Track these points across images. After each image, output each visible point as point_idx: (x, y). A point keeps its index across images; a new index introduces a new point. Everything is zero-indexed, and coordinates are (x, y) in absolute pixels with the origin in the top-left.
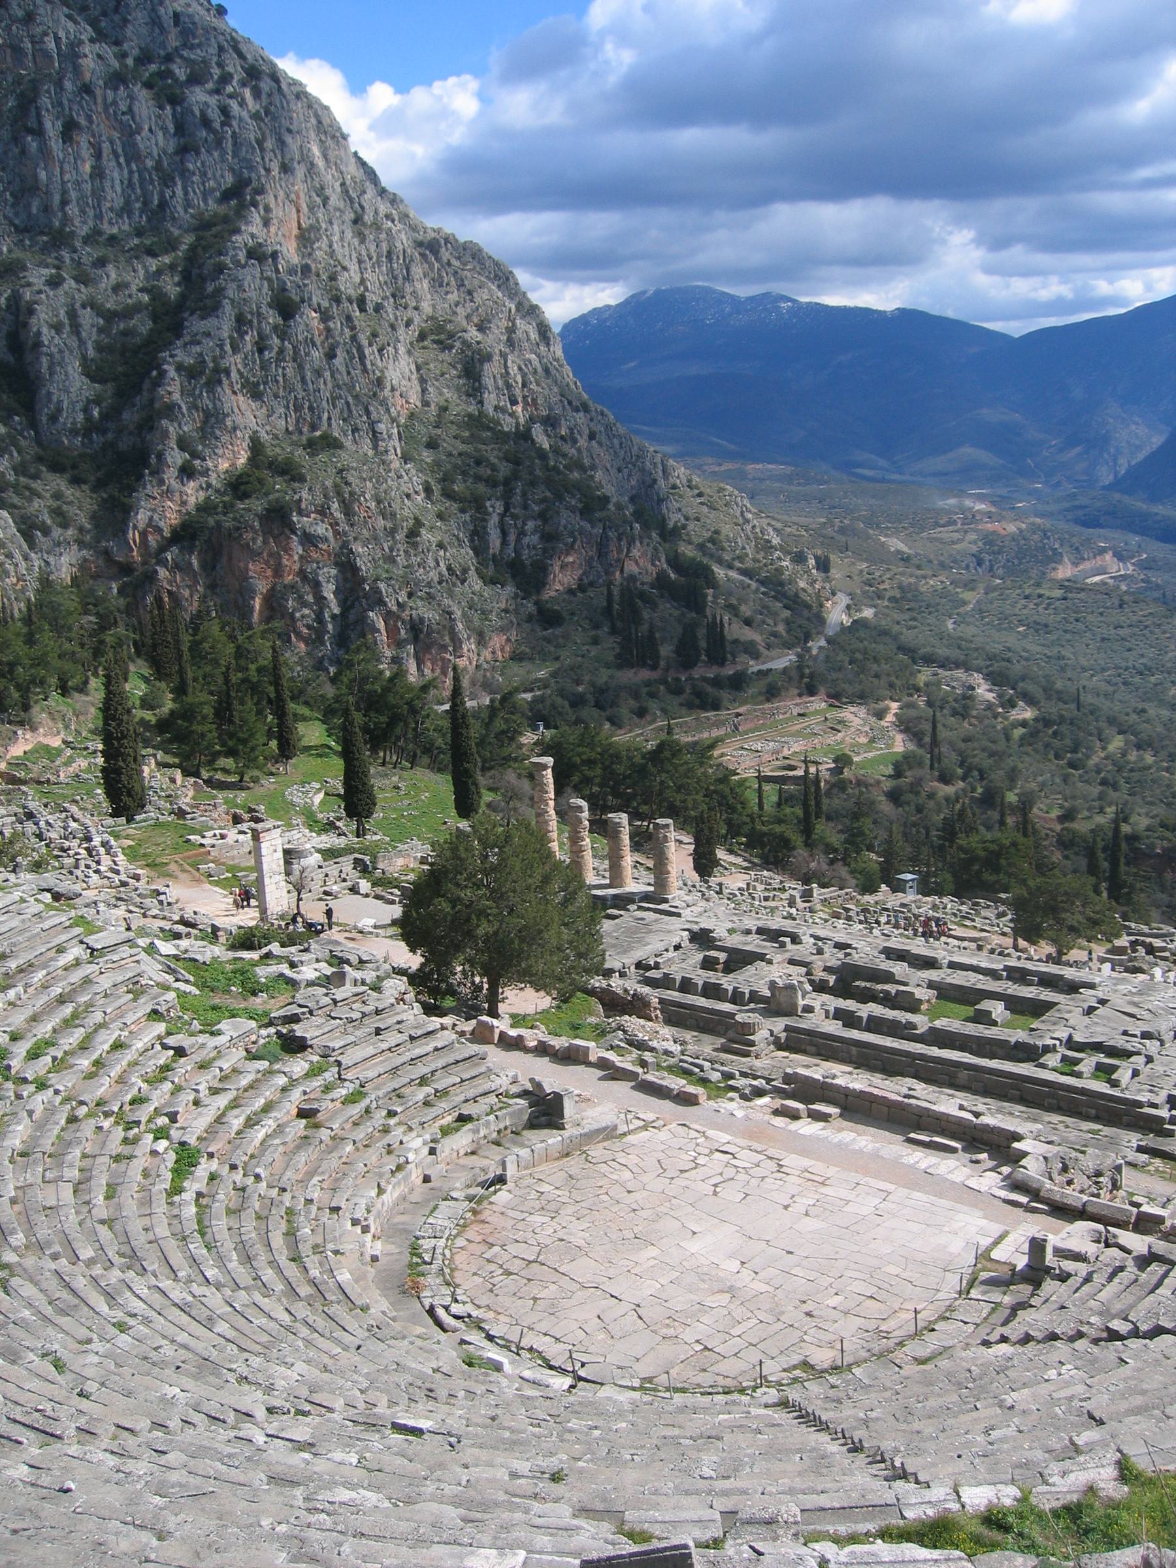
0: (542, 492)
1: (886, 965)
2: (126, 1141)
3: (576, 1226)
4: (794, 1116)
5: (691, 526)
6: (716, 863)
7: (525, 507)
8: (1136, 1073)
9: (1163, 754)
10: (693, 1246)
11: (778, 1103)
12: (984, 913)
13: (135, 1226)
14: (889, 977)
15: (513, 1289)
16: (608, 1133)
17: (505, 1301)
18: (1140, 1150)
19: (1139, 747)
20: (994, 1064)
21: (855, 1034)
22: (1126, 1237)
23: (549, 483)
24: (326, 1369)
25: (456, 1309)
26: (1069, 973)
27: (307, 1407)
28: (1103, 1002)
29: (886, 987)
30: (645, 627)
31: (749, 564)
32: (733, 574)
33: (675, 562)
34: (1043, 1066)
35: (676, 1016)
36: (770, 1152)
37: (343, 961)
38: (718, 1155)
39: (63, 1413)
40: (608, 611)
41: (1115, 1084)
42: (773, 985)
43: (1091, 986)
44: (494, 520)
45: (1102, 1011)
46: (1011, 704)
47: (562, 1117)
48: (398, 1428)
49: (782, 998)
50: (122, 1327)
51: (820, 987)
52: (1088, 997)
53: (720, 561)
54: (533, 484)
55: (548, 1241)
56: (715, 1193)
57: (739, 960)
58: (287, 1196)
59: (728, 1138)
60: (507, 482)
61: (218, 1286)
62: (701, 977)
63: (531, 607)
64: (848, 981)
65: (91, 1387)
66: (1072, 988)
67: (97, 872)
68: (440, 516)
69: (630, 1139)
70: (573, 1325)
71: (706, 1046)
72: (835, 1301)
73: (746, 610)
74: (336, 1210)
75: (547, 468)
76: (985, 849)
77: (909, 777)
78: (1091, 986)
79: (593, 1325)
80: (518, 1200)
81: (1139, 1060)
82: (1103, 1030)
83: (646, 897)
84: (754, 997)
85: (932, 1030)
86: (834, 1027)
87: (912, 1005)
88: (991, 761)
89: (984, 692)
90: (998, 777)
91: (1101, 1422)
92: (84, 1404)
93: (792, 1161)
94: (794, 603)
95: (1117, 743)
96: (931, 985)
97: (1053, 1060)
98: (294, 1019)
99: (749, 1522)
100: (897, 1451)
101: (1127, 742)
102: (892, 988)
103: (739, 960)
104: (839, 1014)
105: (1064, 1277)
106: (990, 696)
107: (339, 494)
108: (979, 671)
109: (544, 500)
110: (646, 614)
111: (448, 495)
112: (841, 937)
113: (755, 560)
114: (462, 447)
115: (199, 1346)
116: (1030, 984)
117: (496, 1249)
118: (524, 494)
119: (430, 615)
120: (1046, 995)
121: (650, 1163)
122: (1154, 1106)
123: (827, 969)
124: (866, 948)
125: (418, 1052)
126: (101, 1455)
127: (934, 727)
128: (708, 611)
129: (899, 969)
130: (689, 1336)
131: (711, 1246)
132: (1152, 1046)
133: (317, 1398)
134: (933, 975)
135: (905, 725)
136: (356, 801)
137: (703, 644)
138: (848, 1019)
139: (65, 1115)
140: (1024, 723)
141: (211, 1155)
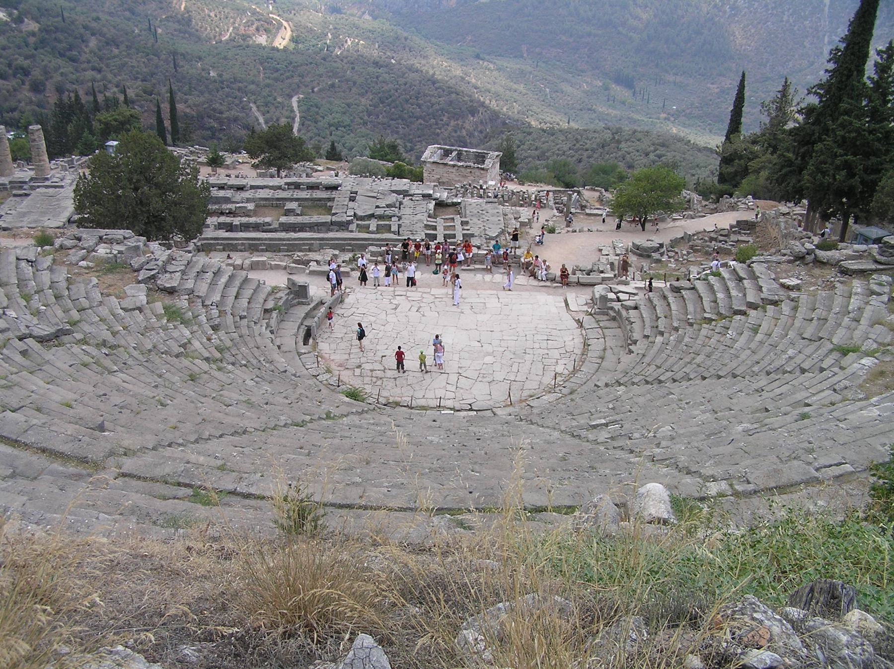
1: (222, 193)
8: (399, 226)
9: (123, 47)
14: (227, 200)
19: (107, 44)
20: (331, 235)
28: (356, 193)
29: (229, 206)
34: (352, 231)
41: (394, 233)
47: (306, 297)
72: (537, 346)
76: (115, 120)
82: (363, 207)
83: (32, 179)
85: (281, 224)
86: (223, 234)
88: (28, 61)
95: (93, 43)
96: (248, 200)
97: (353, 227)
98: (153, 277)
101: (100, 41)
104: (220, 226)
116: (303, 190)
120: (323, 195)
130: (499, 376)
138: (230, 228)
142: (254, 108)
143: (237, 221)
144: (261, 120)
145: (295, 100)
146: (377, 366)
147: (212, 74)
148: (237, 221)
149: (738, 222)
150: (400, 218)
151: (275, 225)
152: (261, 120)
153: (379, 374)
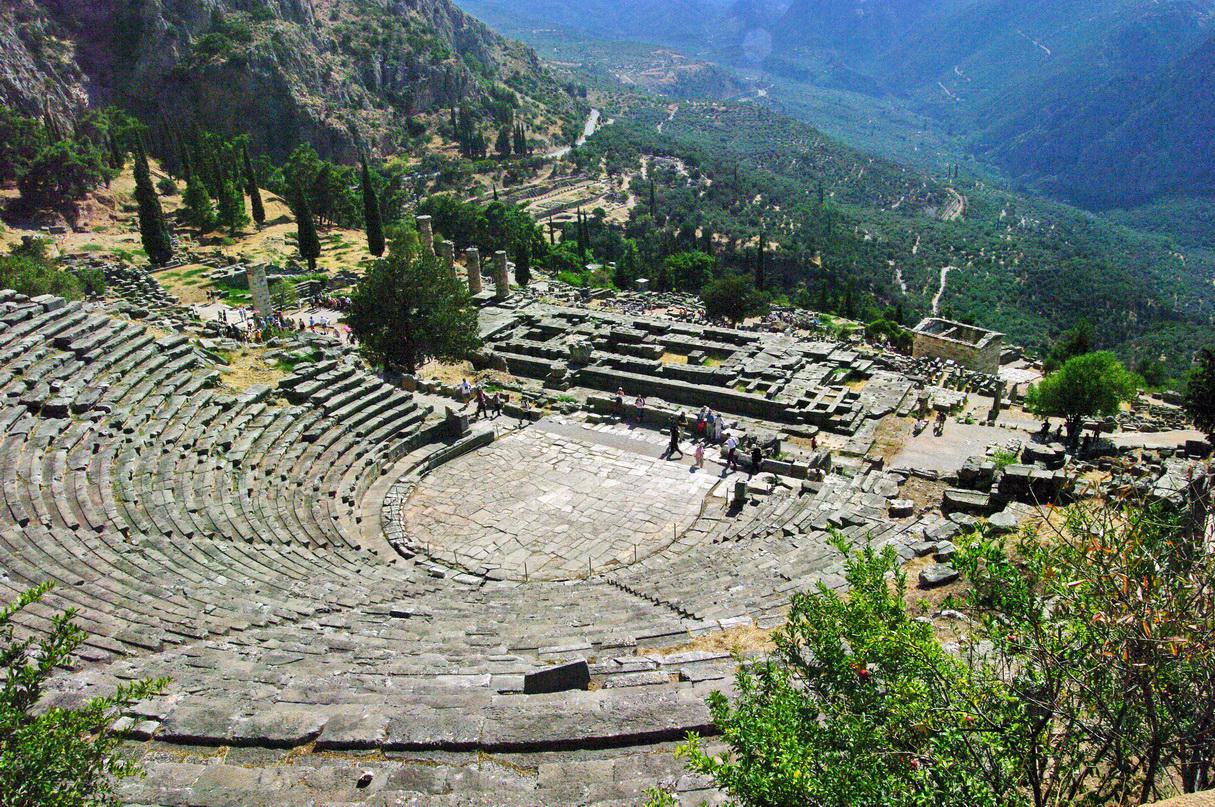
0: (407, 48)
2: (200, 462)
3: (475, 492)
4: (595, 422)
5: (501, 68)
6: (530, 276)
7: (397, 59)
8: (780, 389)
10: (544, 499)
11: (585, 415)
12: (689, 300)
13: (214, 511)
14: (638, 340)
15: (442, 531)
16: (487, 439)
17: (440, 538)
18: (783, 431)
21: (621, 373)
22: (786, 480)
23: (410, 41)
24: (343, 585)
25: (410, 545)
26: (741, 333)
27: (338, 607)
28: (760, 349)
30: (476, 132)
31: (537, 93)
32: (528, 99)
33: (493, 92)
34: (728, 387)
35: (517, 369)
36: (584, 443)
37: (318, 346)
38: (553, 447)
39: (197, 623)
40: (452, 122)
42: (571, 347)
43: (755, 340)
44: (377, 66)
45: (760, 354)
46: (695, 176)
48: (395, 614)
49: (578, 354)
50: (220, 573)
51: (599, 347)
52: (752, 346)
53: (521, 92)
54: (400, 42)
55: (460, 502)
56: (555, 469)
57: (548, 333)
58: (302, 488)
59: (557, 437)
60: (385, 43)
61: (270, 543)
62: (527, 344)
63: (403, 120)
64: (614, 342)
65: (209, 607)
66: (742, 342)
67: (146, 298)
68: (344, 64)
69: (502, 440)
70: (478, 551)
71: (534, 385)
72: (628, 525)
73: (537, 122)
74: (332, 494)
75: (408, 31)
77: (639, 221)
78: (755, 340)
79: (491, 548)
80: (439, 481)
81: (783, 380)
84: (559, 355)
86: (606, 370)
87: (654, 356)
89: (680, 166)
90: (690, 220)
91: (789, 580)
92: (209, 618)
93: (596, 448)
94: (567, 117)
96: (662, 343)
99: (608, 647)
100: (679, 603)
102: (640, 346)
103: (548, 333)
105: (755, 503)
106: (685, 173)
107: (276, 50)
108: (678, 156)
109: (409, 53)
110: (477, 125)
111: (348, 50)
112: (608, 317)
113: (541, 90)
114: (354, 19)
115: (267, 579)
117: (430, 510)
118: (396, 51)
119: (342, 127)
121: (515, 453)
122: (793, 407)
123: (602, 337)
124: (625, 320)
125: (371, 396)
126: (228, 646)
127: (652, 191)
128: (515, 123)
129: (640, 333)
130: (548, 549)
131: (556, 498)
132: (789, 373)
133: (342, 602)
134: (664, 338)
135: (635, 188)
136: (308, 246)
137: (512, 143)
138: (616, 365)
139: (160, 449)
140: (705, 188)
141: (253, 468)
142: (899, 275)
143: (625, 359)
144: (904, 287)
145: (944, 271)
146: (450, 510)
147: (867, 237)
148: (625, 359)
149: (1188, 442)
150: (788, 381)
151: (660, 369)
152: (904, 287)
153: (443, 517)
